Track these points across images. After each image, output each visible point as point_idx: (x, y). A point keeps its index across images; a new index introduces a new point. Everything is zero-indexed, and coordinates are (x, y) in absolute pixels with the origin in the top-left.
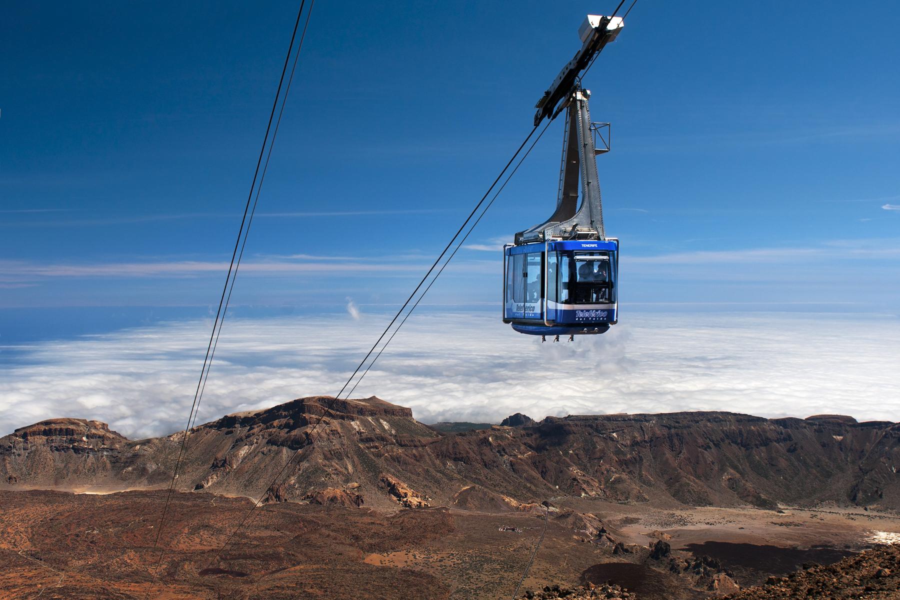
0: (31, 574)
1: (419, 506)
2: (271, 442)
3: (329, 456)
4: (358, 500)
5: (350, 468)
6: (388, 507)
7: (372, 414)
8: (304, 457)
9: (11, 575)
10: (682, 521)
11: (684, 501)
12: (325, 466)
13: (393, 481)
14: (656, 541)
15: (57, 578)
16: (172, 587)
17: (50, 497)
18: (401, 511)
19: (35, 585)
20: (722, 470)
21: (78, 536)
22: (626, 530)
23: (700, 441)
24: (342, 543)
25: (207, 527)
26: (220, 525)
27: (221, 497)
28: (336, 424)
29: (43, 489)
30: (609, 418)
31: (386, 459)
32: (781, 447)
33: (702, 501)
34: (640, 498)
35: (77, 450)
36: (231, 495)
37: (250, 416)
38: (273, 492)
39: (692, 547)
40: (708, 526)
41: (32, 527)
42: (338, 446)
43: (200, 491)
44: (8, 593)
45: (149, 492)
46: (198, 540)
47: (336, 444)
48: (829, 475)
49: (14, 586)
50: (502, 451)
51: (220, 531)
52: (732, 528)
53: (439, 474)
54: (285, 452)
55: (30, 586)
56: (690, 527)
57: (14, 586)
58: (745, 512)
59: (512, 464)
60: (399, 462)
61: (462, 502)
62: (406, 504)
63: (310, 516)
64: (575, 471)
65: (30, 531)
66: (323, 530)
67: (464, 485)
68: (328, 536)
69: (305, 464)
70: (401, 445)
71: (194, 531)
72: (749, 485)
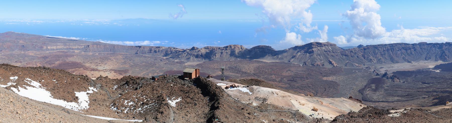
4: (323, 65)
7: (327, 46)
10: (393, 67)
11: (393, 62)
13: (331, 60)
20: (401, 55)
23: (397, 49)
28: (319, 48)
30: (379, 45)
32: (413, 50)
33: (397, 62)
34: (384, 62)
47: (319, 52)
48: (422, 55)
50: (355, 53)
52: (402, 68)
59: (357, 56)
61: (346, 65)
63: (312, 69)
64: (371, 57)
66: (314, 72)
69: (312, 57)
71: (287, 71)
72: (407, 58)
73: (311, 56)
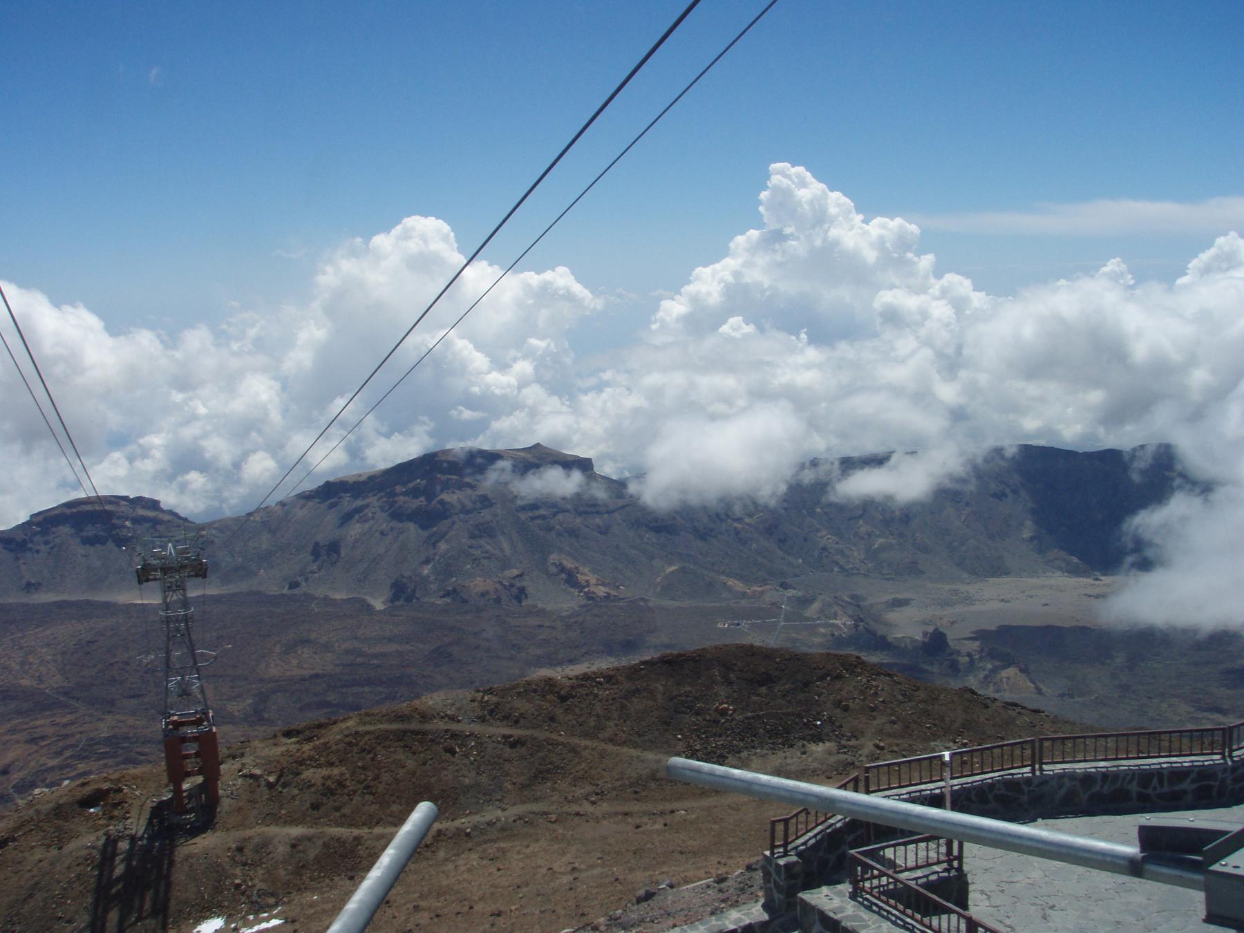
0: (65, 720)
1: (608, 597)
2: (397, 516)
3: (477, 532)
4: (521, 594)
5: (506, 546)
6: (565, 602)
8: (442, 536)
9: (38, 723)
10: (968, 600)
12: (471, 547)
13: (569, 564)
14: (930, 629)
15: (101, 725)
16: (262, 729)
17: (84, 609)
18: (582, 606)
19: (72, 735)
21: (127, 663)
22: (893, 616)
24: (498, 657)
25: (306, 642)
26: (325, 639)
27: (326, 598)
29: (73, 598)
31: (559, 534)
33: (998, 569)
35: (120, 542)
36: (338, 596)
37: (361, 479)
38: (401, 591)
39: (981, 635)
40: (1001, 605)
41: (63, 653)
42: (488, 518)
43: (296, 591)
44: (35, 748)
45: (222, 596)
46: (295, 662)
47: (486, 515)
49: (43, 738)
51: (327, 647)
53: (633, 551)
54: (412, 527)
55: (66, 736)
56: (978, 607)
57: (43, 738)
58: (1052, 582)
60: (577, 537)
62: (590, 597)
65: (59, 658)
67: (670, 564)
68: (478, 647)
69: (443, 546)
70: (580, 514)
71: (290, 648)
73: (433, 542)
